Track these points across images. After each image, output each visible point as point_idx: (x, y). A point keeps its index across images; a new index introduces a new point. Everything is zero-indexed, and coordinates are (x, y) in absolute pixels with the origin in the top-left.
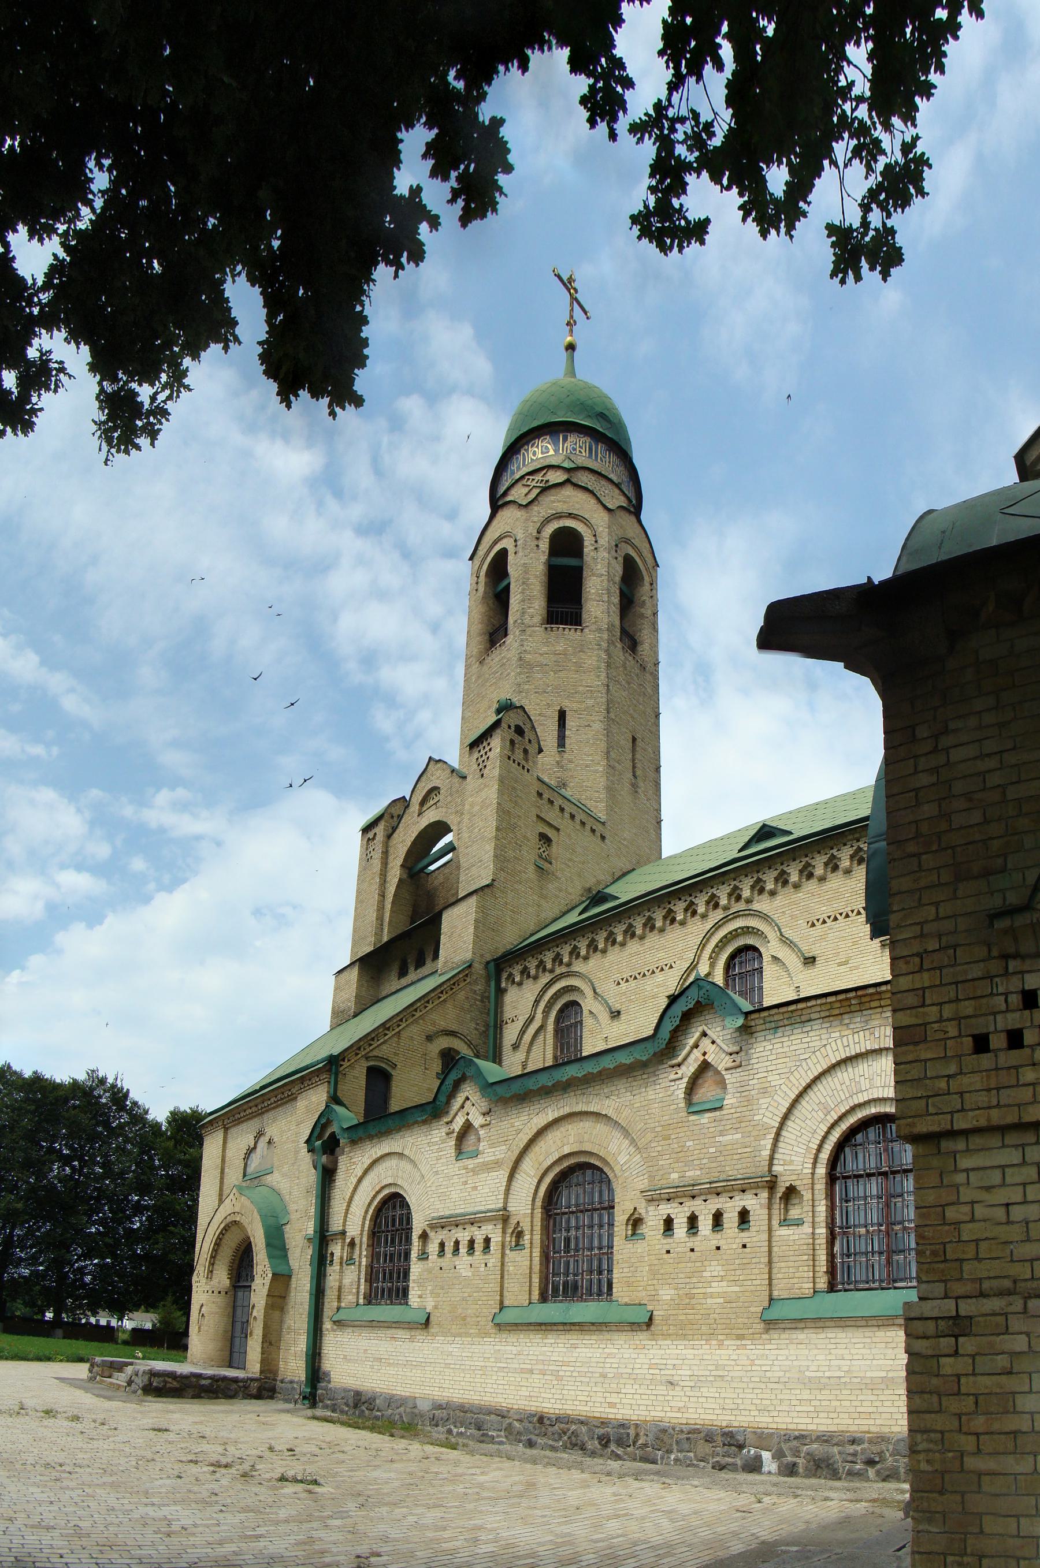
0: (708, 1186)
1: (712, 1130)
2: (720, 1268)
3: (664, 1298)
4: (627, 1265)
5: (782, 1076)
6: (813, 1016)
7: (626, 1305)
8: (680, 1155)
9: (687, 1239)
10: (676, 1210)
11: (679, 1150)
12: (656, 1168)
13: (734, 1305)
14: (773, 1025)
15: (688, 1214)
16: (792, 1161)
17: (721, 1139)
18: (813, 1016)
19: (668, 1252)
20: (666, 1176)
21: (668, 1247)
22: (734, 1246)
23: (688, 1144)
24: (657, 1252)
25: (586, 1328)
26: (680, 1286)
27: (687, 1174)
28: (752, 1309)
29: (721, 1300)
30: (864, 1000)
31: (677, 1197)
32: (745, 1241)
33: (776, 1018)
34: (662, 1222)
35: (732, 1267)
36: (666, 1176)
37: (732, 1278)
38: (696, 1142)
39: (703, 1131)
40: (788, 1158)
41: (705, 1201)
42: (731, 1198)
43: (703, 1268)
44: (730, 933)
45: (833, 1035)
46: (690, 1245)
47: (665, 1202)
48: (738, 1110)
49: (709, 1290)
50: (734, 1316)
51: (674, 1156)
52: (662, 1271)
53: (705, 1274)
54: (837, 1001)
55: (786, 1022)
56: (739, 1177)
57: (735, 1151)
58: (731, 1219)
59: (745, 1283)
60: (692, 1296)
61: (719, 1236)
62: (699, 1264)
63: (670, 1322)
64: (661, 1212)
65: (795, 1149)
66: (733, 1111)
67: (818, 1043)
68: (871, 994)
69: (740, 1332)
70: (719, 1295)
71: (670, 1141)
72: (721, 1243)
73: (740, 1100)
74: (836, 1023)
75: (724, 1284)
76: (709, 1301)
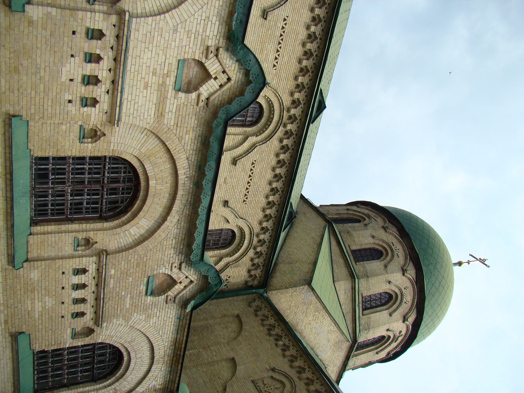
0: (102, 297)
1: (135, 291)
2: (50, 305)
3: (32, 274)
4: (57, 240)
5: (154, 324)
6: (179, 336)
7: (28, 242)
8: (125, 275)
9: (70, 284)
10: (90, 276)
11: (128, 274)
12: (120, 259)
13: (27, 316)
14: (182, 318)
15: (87, 283)
16: (108, 330)
17: (129, 297)
18: (179, 336)
19: (63, 273)
20: (114, 266)
21: (66, 273)
22: (63, 312)
23: (131, 279)
24: (64, 266)
25: (9, 218)
26: (40, 283)
27: (112, 280)
28: (24, 326)
29: (30, 309)
30: (178, 357)
31: (99, 277)
32: (66, 318)
33: (184, 321)
34: (84, 267)
35: (50, 312)
36: (114, 266)
37: (44, 313)
38: (130, 283)
39: (136, 287)
40: (110, 328)
41: (93, 292)
42: (93, 306)
43: (51, 296)
44: (274, 110)
45: (167, 343)
46: (67, 286)
47: (97, 268)
48: (142, 305)
49: (36, 301)
50: (20, 317)
51: (125, 272)
52: (50, 271)
53: (47, 298)
54: (181, 348)
55: (181, 324)
56: (104, 309)
57: (119, 306)
58: (81, 308)
59: (40, 321)
60: (33, 291)
61: (71, 302)
62: (54, 293)
63: (15, 280)
64: (91, 266)
65: (114, 331)
66: (143, 302)
67: (165, 337)
68: (179, 360)
69: (10, 321)
70: (33, 307)
71: (135, 267)
72: (66, 305)
73: (148, 305)
74: (172, 343)
75: (40, 309)
76: (29, 302)
